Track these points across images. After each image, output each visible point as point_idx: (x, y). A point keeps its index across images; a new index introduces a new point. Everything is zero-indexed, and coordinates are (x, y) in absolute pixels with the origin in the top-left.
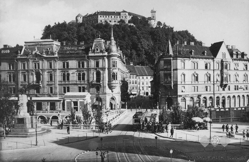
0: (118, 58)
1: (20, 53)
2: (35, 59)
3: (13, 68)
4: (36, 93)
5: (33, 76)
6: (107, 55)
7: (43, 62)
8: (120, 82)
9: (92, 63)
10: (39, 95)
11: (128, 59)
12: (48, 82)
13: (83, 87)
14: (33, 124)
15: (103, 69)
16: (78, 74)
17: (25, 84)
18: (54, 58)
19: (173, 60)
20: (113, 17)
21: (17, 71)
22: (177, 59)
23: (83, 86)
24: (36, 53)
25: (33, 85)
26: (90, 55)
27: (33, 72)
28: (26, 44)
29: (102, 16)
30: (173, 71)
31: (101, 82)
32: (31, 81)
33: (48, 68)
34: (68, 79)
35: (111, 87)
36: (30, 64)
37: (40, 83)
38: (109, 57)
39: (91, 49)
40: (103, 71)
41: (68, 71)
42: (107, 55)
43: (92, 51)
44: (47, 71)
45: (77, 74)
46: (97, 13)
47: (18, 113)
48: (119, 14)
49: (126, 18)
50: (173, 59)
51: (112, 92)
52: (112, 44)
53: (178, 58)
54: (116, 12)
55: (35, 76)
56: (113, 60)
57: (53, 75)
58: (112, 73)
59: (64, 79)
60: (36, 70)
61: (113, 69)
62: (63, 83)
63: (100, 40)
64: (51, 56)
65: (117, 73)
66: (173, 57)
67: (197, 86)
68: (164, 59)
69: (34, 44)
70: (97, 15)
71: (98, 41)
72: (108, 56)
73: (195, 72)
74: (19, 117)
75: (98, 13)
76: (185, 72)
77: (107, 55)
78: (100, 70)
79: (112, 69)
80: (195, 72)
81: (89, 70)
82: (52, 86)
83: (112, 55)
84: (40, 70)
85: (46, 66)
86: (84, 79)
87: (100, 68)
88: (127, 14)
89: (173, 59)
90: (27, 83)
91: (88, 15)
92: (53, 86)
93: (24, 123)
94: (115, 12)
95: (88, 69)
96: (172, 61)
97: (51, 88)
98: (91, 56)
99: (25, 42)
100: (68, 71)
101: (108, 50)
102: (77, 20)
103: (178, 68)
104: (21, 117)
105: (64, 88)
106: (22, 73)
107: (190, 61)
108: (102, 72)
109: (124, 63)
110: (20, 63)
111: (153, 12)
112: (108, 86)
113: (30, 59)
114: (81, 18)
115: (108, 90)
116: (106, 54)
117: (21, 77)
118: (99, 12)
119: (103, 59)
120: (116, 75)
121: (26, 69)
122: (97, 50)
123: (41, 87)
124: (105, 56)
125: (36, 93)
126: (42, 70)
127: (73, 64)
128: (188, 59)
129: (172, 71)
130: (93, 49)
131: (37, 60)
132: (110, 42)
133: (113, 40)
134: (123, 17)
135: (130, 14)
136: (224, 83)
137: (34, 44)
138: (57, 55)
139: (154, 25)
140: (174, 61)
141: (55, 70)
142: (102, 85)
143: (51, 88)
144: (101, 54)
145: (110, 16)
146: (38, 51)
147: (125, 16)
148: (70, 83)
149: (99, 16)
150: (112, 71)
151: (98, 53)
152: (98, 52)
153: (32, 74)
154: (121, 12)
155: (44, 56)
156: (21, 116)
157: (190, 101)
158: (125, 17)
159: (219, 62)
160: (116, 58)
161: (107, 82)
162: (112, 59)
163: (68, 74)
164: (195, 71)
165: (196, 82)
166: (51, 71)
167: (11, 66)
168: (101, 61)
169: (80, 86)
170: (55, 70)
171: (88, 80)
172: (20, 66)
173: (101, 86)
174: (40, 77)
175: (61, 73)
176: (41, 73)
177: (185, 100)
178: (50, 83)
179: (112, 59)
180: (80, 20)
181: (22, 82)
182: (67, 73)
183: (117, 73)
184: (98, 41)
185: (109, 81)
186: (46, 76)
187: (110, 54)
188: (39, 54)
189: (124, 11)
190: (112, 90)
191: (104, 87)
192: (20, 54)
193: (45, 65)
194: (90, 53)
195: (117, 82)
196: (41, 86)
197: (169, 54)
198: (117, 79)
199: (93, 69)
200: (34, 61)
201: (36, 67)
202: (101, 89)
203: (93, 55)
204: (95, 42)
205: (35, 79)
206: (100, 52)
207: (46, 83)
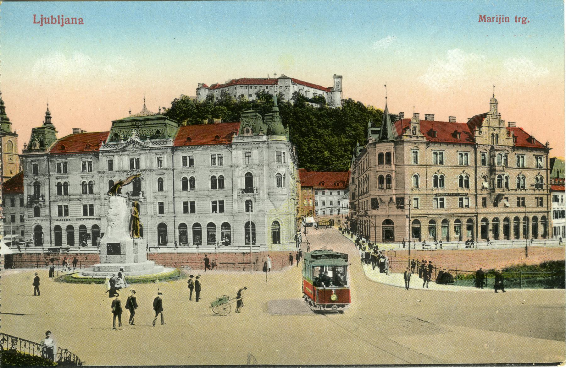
18: (167, 148)
102: (198, 94)
116: (265, 138)
118: (237, 79)
136: (498, 191)
142: (256, 196)
159: (485, 151)
160: (284, 146)
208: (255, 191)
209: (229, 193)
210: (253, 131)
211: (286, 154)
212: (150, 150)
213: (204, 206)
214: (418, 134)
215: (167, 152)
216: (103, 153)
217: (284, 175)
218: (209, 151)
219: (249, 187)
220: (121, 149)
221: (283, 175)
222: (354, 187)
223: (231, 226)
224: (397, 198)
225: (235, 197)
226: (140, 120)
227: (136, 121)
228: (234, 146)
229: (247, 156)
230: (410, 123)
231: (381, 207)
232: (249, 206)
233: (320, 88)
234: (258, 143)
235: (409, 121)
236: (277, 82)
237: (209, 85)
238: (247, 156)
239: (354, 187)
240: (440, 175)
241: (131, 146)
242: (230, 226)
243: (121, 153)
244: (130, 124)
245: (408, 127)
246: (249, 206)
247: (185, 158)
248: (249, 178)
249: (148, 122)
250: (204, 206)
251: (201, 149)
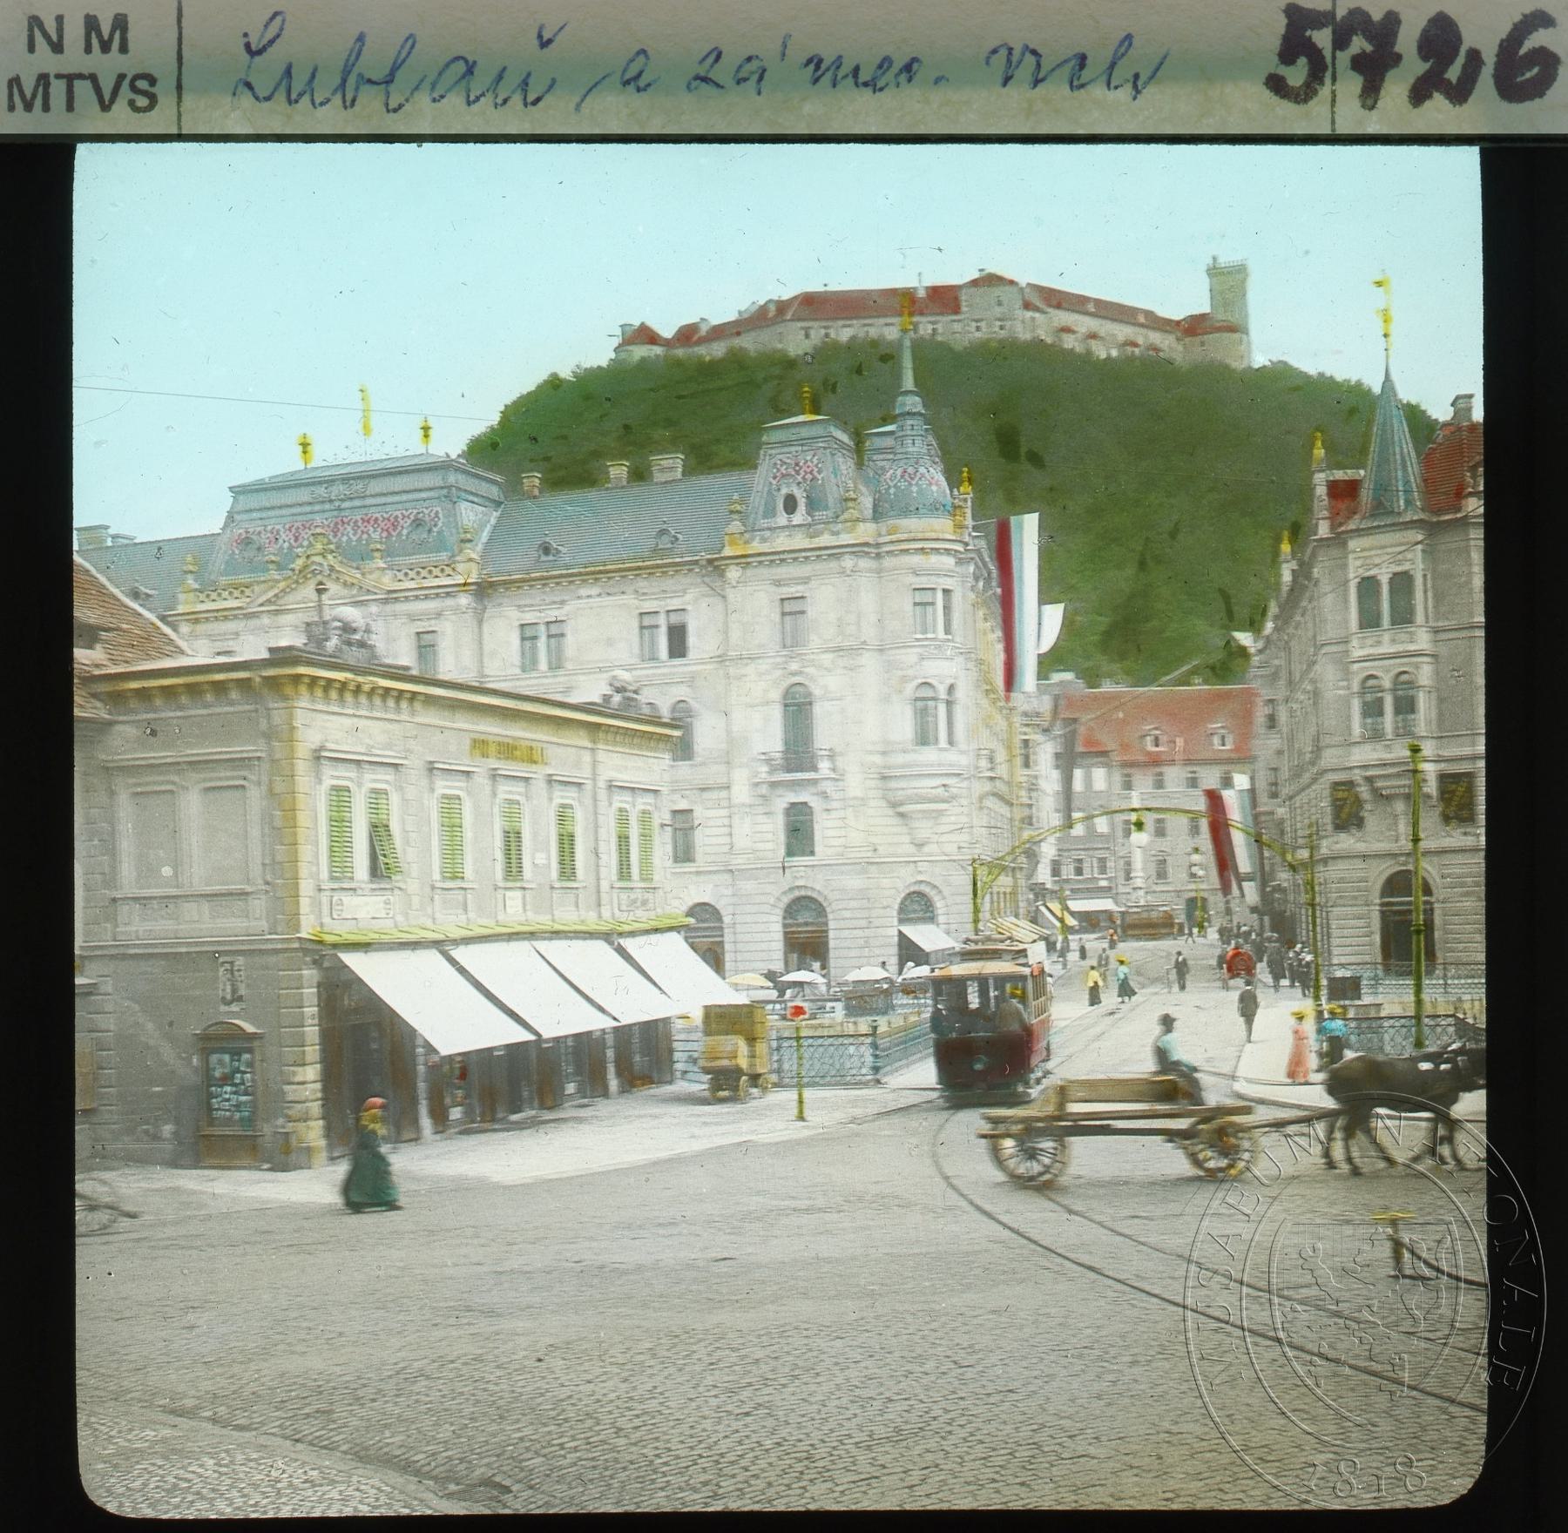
173: (824, 795)
183: (951, 688)
208: (824, 765)
209: (714, 774)
210: (812, 505)
211: (957, 598)
212: (386, 601)
215: (457, 610)
216: (197, 621)
217: (951, 688)
218: (629, 599)
219: (799, 752)
220: (269, 601)
222: (1274, 742)
223: (727, 920)
224: (1443, 778)
225: (741, 793)
226: (346, 479)
227: (330, 482)
228: (733, 573)
229: (792, 610)
231: (1372, 822)
232: (799, 834)
233: (1155, 322)
234: (835, 553)
238: (792, 610)
239: (1274, 742)
241: (308, 591)
242: (720, 919)
243: (266, 620)
244: (304, 495)
246: (799, 834)
247: (527, 635)
248: (798, 710)
249: (375, 486)
251: (595, 591)
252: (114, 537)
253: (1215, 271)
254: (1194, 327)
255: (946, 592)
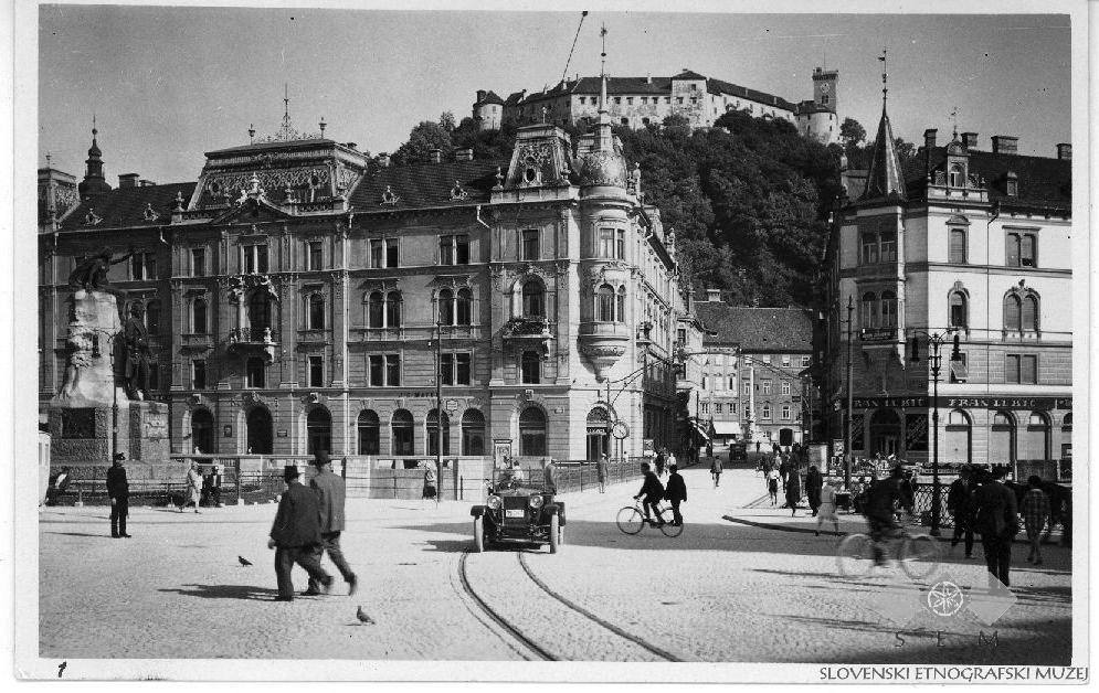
0: (631, 215)
1: (185, 205)
2: (249, 229)
3: (150, 275)
4: (246, 387)
5: (237, 306)
6: (578, 198)
7: (283, 240)
8: (638, 337)
9: (507, 241)
10: (261, 394)
11: (699, 276)
12: (303, 333)
13: (462, 357)
14: (142, 440)
15: (559, 266)
16: (442, 293)
17: (200, 342)
18: (333, 218)
19: (903, 219)
20: (637, 100)
21: (166, 283)
22: (925, 214)
23: (463, 351)
24: (251, 202)
25: (238, 346)
26: (496, 200)
27: (239, 287)
28: (213, 163)
29: (588, 98)
30: (905, 272)
31: (546, 332)
32: (226, 327)
33: (306, 268)
34: (394, 320)
35: (591, 353)
36: (225, 249)
37: (268, 339)
38: (586, 210)
39: (505, 171)
40: (556, 278)
41: (396, 280)
42: (578, 198)
43: (508, 184)
44: (299, 283)
45: (437, 295)
46: (565, 87)
47: (69, 389)
48: (664, 86)
49: (695, 102)
50: (905, 217)
51: (600, 380)
52: (603, 148)
53: (931, 209)
54: (649, 82)
55: (243, 312)
56: (607, 225)
57: (327, 299)
58: (598, 286)
59: (376, 320)
60: (252, 277)
61: (603, 270)
62: (369, 338)
63: (549, 133)
64: (319, 213)
65: (622, 287)
66: (905, 206)
67: (1034, 356)
68: (862, 213)
69: (247, 159)
70: (568, 94)
71: (542, 134)
72: (581, 202)
73: (1022, 283)
74: (75, 404)
75: (570, 85)
76: (971, 281)
77: (573, 200)
78: (541, 275)
79: (598, 269)
80: (1022, 283)
81: (493, 274)
82: (316, 354)
83: (603, 199)
84: (267, 277)
85: (295, 250)
86: (465, 318)
87: (542, 265)
88: (701, 85)
89: (905, 217)
90: (209, 341)
91: (526, 95)
92: (325, 355)
93: (94, 437)
94: (645, 80)
95: (487, 273)
96: (900, 224)
97: (317, 362)
98: (500, 207)
99: (210, 156)
100: (396, 280)
101: (586, 177)
103: (931, 259)
104: (83, 405)
105: (377, 360)
106: (190, 294)
107: (997, 225)
108: (550, 282)
109: (670, 265)
110: (183, 251)
111: (824, 77)
112: (580, 351)
113: (224, 228)
114: (494, 109)
115: (575, 370)
116: (573, 193)
117: (183, 313)
118: (573, 79)
119: (559, 217)
120: (621, 299)
121: (208, 271)
122: (531, 176)
123: (270, 356)
124: (568, 203)
125: (250, 385)
126: (275, 279)
127: (419, 248)
128: (984, 213)
129: (901, 274)
130: (511, 172)
131: (256, 232)
132: (592, 142)
133: (609, 130)
134: (681, 99)
135: (716, 87)
137: (247, 159)
138: (345, 207)
139: (826, 136)
140: (911, 222)
141: (333, 278)
142: (549, 343)
143: (317, 362)
144: (551, 197)
145: (624, 99)
146: (262, 190)
147: (693, 94)
148: (403, 338)
149: (575, 99)
150: (597, 277)
151: (536, 190)
152: (533, 185)
153: (234, 299)
154: (675, 78)
155: (290, 213)
156: (80, 397)
157: (996, 428)
158: (694, 100)
160: (623, 214)
161: (574, 330)
162: (602, 219)
163: (396, 297)
164: (1019, 279)
165: (1030, 336)
166: (319, 285)
167: (144, 269)
168: (546, 233)
169: (445, 351)
170: (333, 278)
171: (486, 325)
172: (183, 261)
173: (545, 349)
174: (267, 313)
175: (362, 291)
176: (272, 290)
177: (969, 421)
178: (310, 339)
179: (602, 219)
180: (493, 117)
181: (187, 337)
182: (390, 289)
184: (542, 134)
185: (586, 325)
186: (294, 312)
187: (592, 196)
188: (264, 201)
189: (689, 75)
190: (597, 372)
191: (561, 354)
192: (181, 210)
193: (293, 253)
194: (499, 192)
195: (621, 330)
196: (271, 351)
197: (884, 187)
198: (621, 319)
199: (508, 266)
200: (241, 239)
201: (250, 268)
202: (547, 369)
203: (510, 199)
204: (521, 141)
205: (244, 323)
206: (543, 188)
207: (291, 338)
213: (420, 369)
214: (969, 185)
221: (616, 289)
230: (946, 156)
233: (782, 104)
235: (943, 153)
236: (670, 87)
237: (505, 98)
240: (1027, 293)
245: (943, 167)
250: (420, 369)
252: (143, 182)
253: (819, 77)
254: (806, 109)
255: (619, 231)
